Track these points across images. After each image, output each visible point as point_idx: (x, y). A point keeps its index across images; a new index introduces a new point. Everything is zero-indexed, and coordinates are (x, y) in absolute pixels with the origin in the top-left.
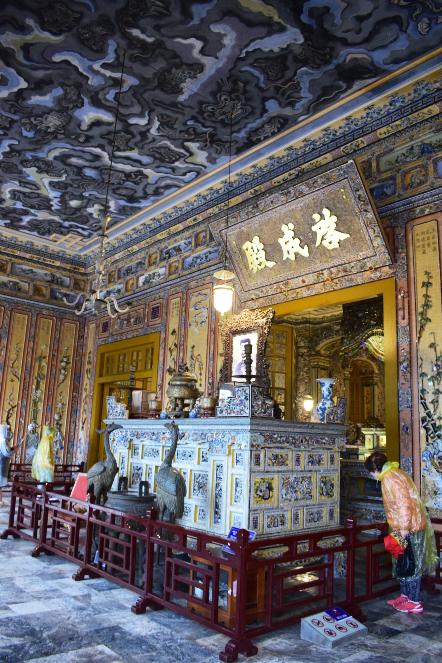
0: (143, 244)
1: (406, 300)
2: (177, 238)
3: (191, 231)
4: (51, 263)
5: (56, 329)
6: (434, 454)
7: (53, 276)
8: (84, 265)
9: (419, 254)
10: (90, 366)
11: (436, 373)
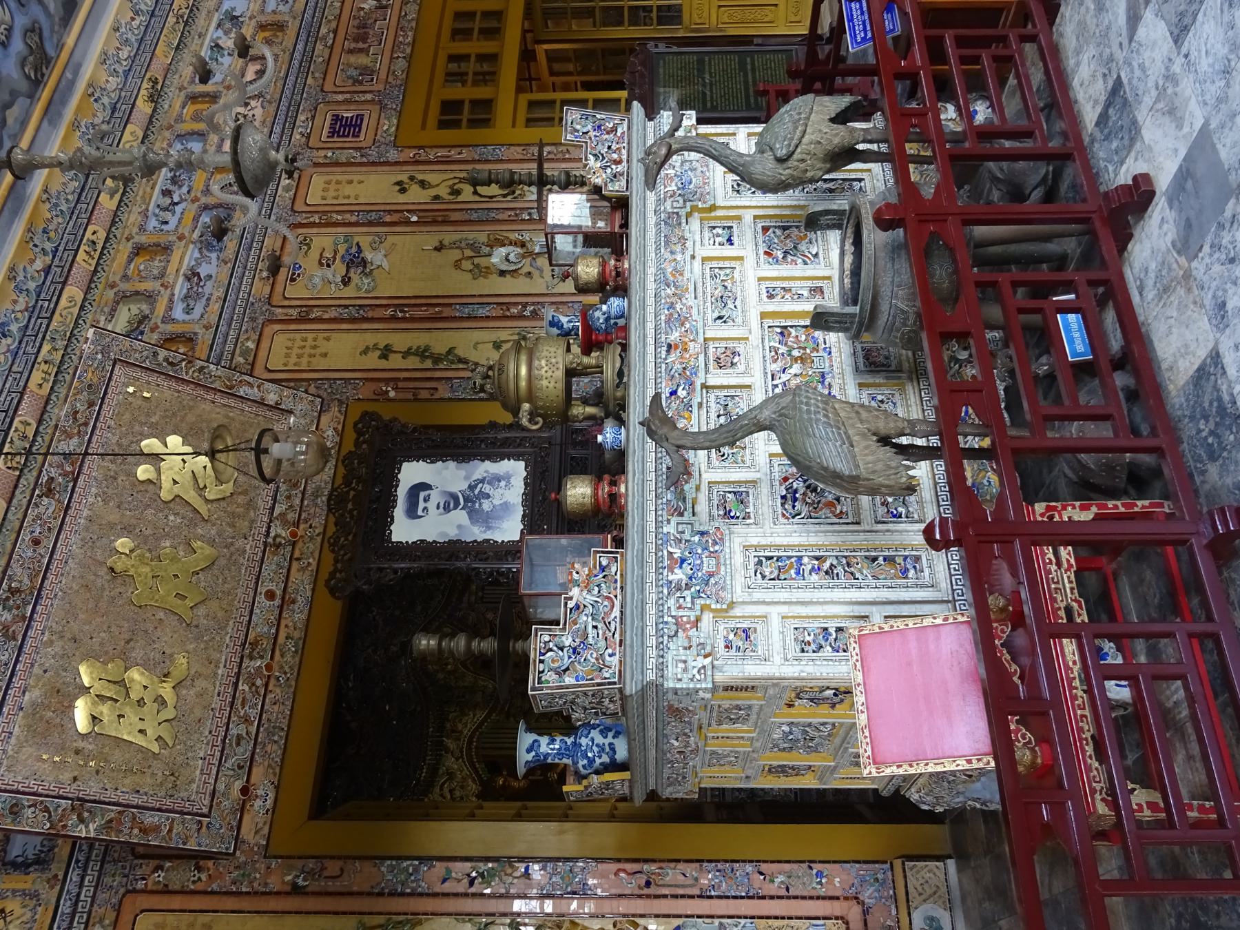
1: (401, 385)
9: (322, 364)
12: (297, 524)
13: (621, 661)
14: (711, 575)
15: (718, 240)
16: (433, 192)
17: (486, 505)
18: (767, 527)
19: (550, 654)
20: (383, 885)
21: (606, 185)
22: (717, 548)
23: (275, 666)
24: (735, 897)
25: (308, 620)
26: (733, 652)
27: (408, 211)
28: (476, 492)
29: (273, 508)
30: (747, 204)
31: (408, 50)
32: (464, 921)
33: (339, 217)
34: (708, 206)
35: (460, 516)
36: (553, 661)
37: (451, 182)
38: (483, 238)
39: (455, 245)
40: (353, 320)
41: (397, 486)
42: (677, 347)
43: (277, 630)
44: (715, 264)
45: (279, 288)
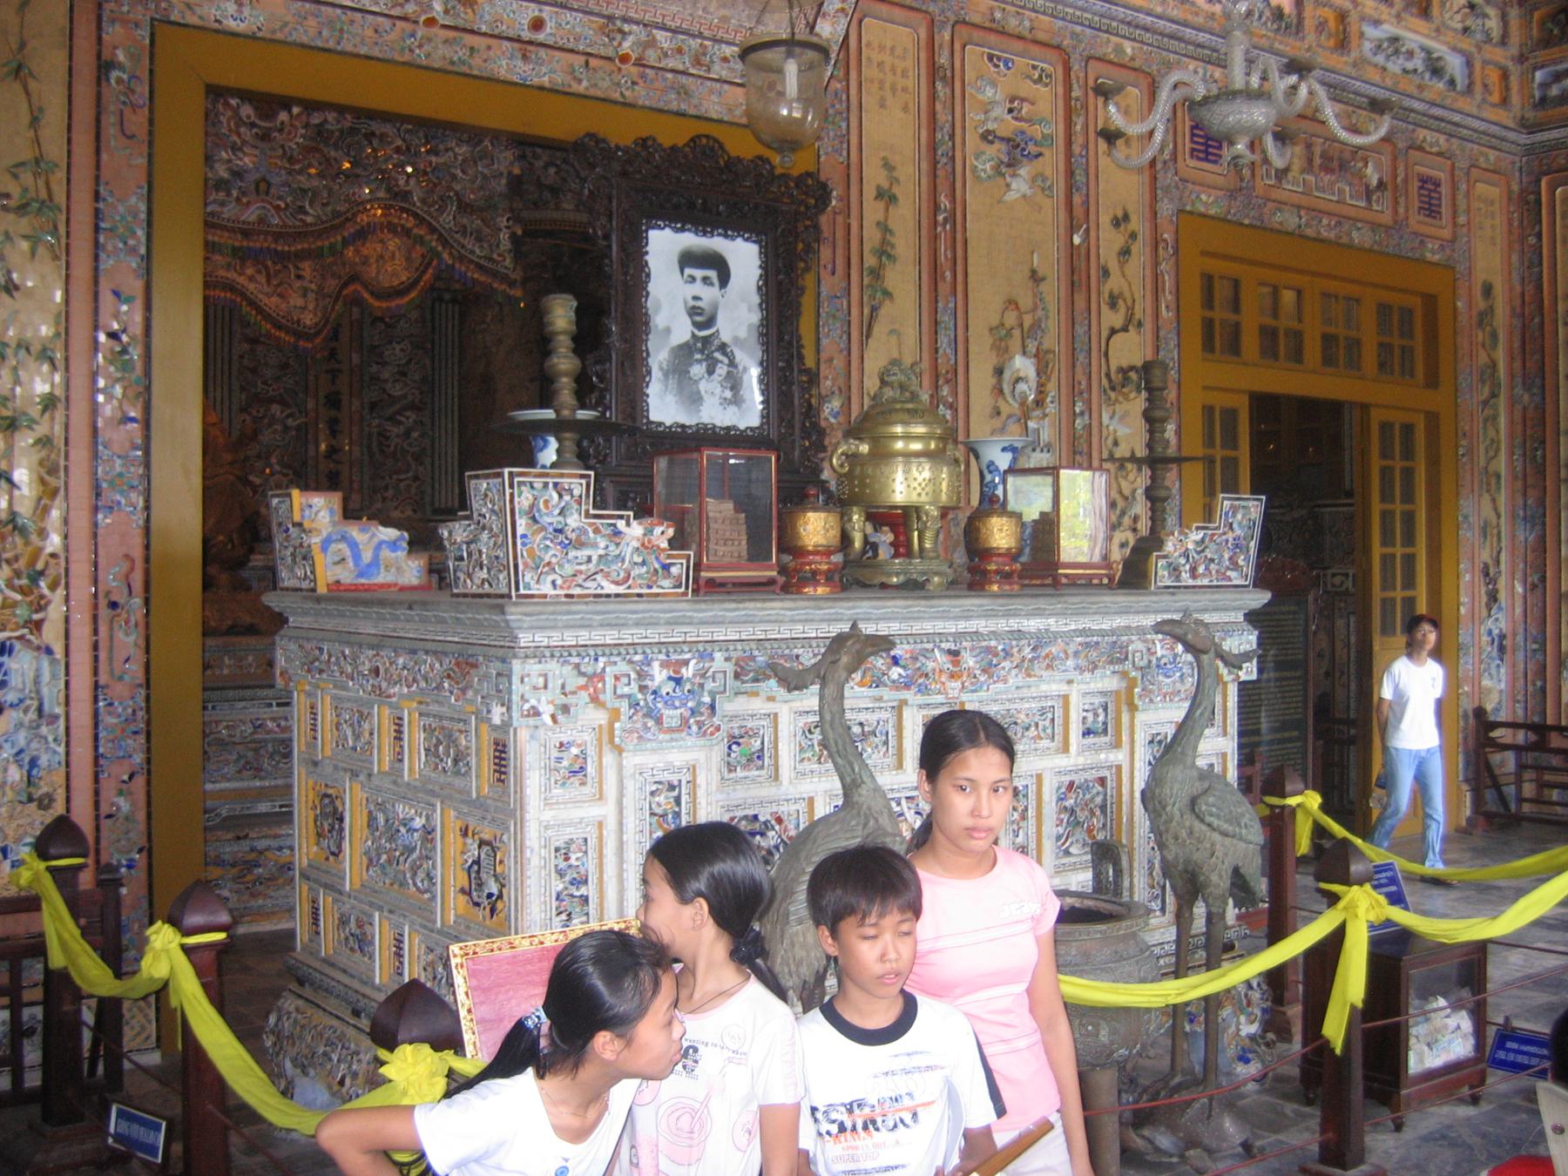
9: (869, 101)
12: (640, 63)
13: (545, 596)
14: (659, 721)
15: (1090, 716)
16: (1113, 266)
17: (698, 370)
18: (721, 797)
19: (555, 496)
20: (110, 200)
21: (1165, 557)
22: (695, 728)
23: (435, 30)
24: (96, 738)
25: (498, 81)
26: (555, 754)
27: (1087, 230)
28: (717, 355)
29: (664, 28)
30: (1137, 756)
31: (1310, 232)
32: (57, 324)
33: (1078, 127)
34: (1136, 701)
35: (683, 331)
36: (546, 502)
37: (1127, 295)
38: (1049, 342)
39: (1039, 298)
40: (933, 147)
41: (726, 236)
42: (956, 663)
43: (485, 34)
44: (1059, 713)
45: (977, 35)
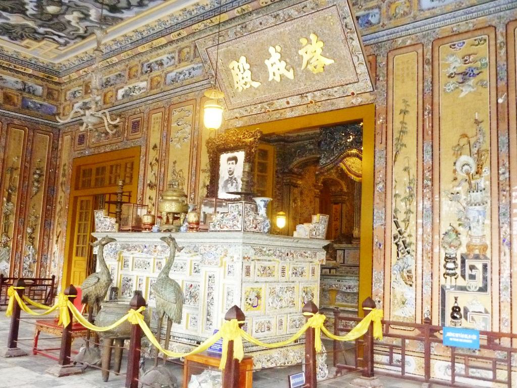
0: (123, 56)
1: (384, 126)
2: (159, 51)
3: (174, 45)
4: (23, 71)
5: (29, 140)
6: (404, 268)
7: (24, 84)
8: (57, 73)
9: (396, 83)
10: (64, 179)
11: (407, 195)
28: (234, 181)
41: (237, 151)
